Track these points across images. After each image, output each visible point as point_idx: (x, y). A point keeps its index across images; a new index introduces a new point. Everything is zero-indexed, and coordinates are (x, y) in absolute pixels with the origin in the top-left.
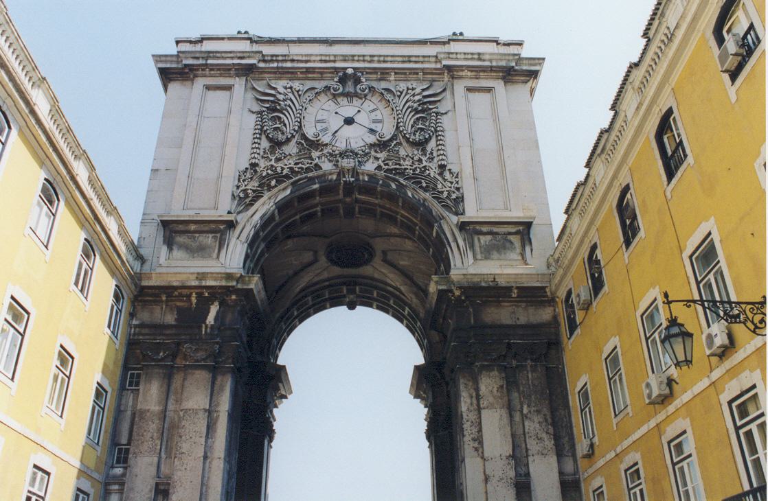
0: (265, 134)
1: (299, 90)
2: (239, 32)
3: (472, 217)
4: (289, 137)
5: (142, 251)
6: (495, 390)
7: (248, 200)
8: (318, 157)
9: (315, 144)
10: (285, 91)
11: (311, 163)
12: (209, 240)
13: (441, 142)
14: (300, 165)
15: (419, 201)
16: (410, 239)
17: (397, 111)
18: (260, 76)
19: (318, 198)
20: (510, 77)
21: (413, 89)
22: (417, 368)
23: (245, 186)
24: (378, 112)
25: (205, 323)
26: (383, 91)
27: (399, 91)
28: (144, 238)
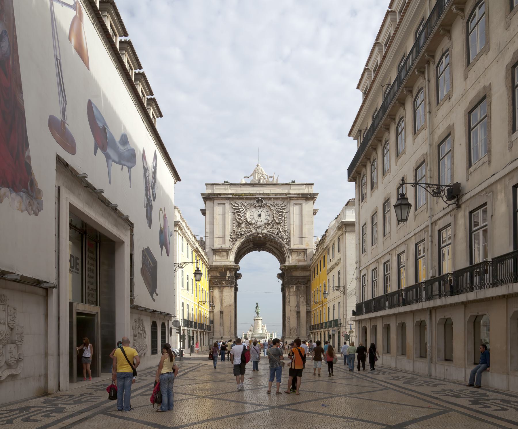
12: (225, 254)
21: (279, 204)
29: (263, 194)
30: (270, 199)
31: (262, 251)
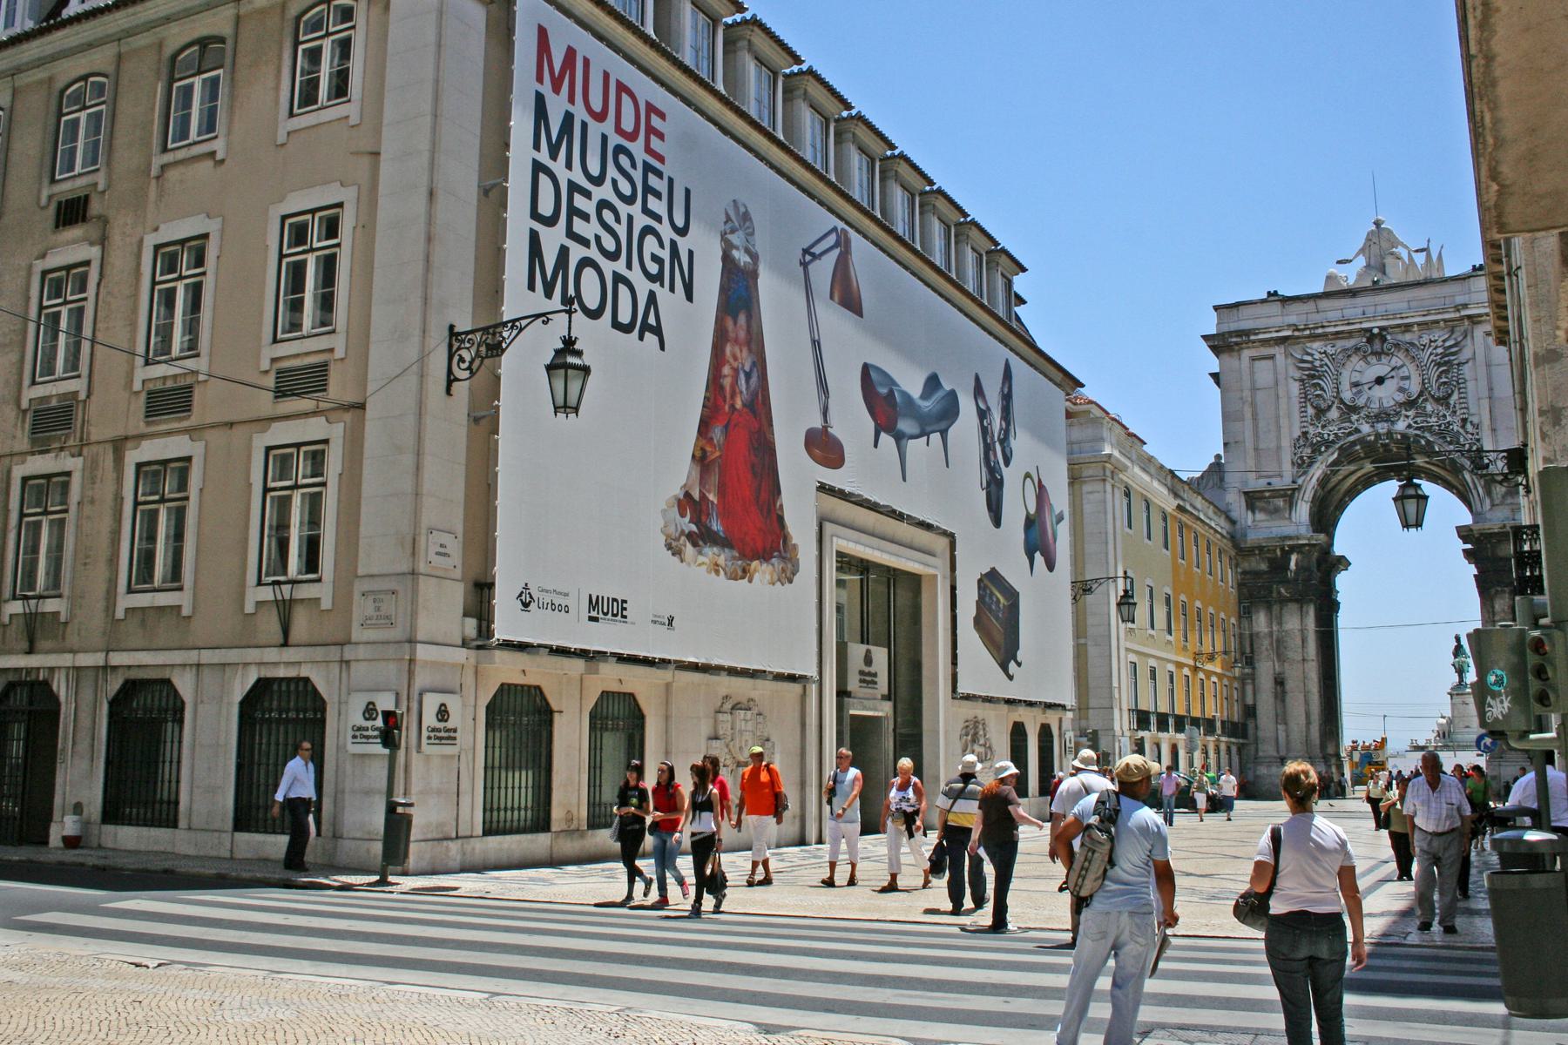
2: (1269, 293)
9: (1354, 409)
12: (1280, 503)
21: (1436, 341)
29: (1385, 317)
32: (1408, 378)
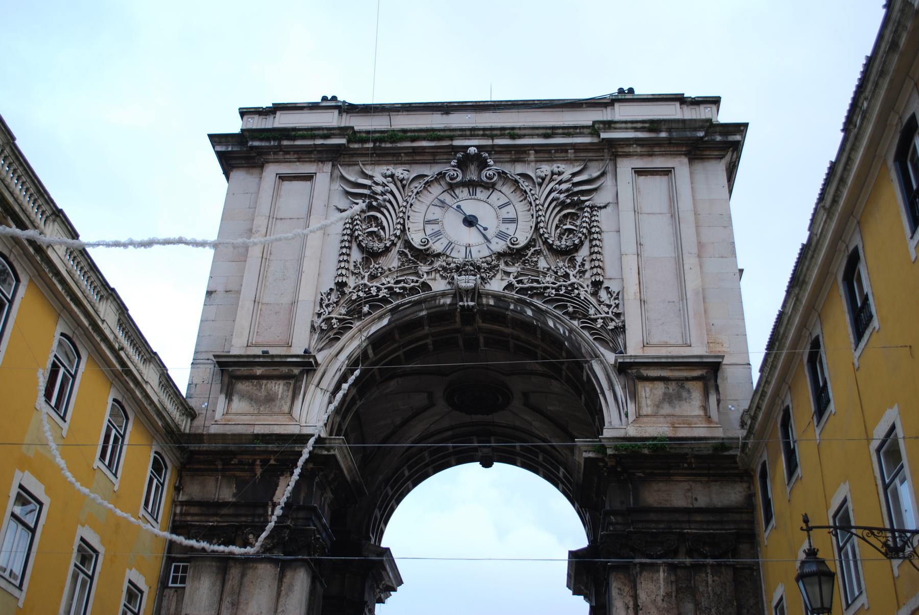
0: (356, 240)
1: (403, 179)
2: (324, 99)
3: (636, 357)
4: (388, 245)
5: (192, 403)
6: (659, 599)
7: (332, 335)
8: (428, 273)
9: (423, 255)
10: (385, 181)
11: (417, 281)
12: (279, 388)
13: (596, 249)
14: (402, 284)
15: (564, 332)
16: (556, 379)
17: (537, 205)
18: (351, 160)
19: (427, 328)
20: (698, 152)
21: (560, 174)
22: (572, 554)
23: (329, 313)
24: (510, 208)
25: (272, 500)
26: (518, 178)
27: (539, 177)
28: (196, 385)
30: (518, 154)
31: (496, 465)
32: (514, 221)
